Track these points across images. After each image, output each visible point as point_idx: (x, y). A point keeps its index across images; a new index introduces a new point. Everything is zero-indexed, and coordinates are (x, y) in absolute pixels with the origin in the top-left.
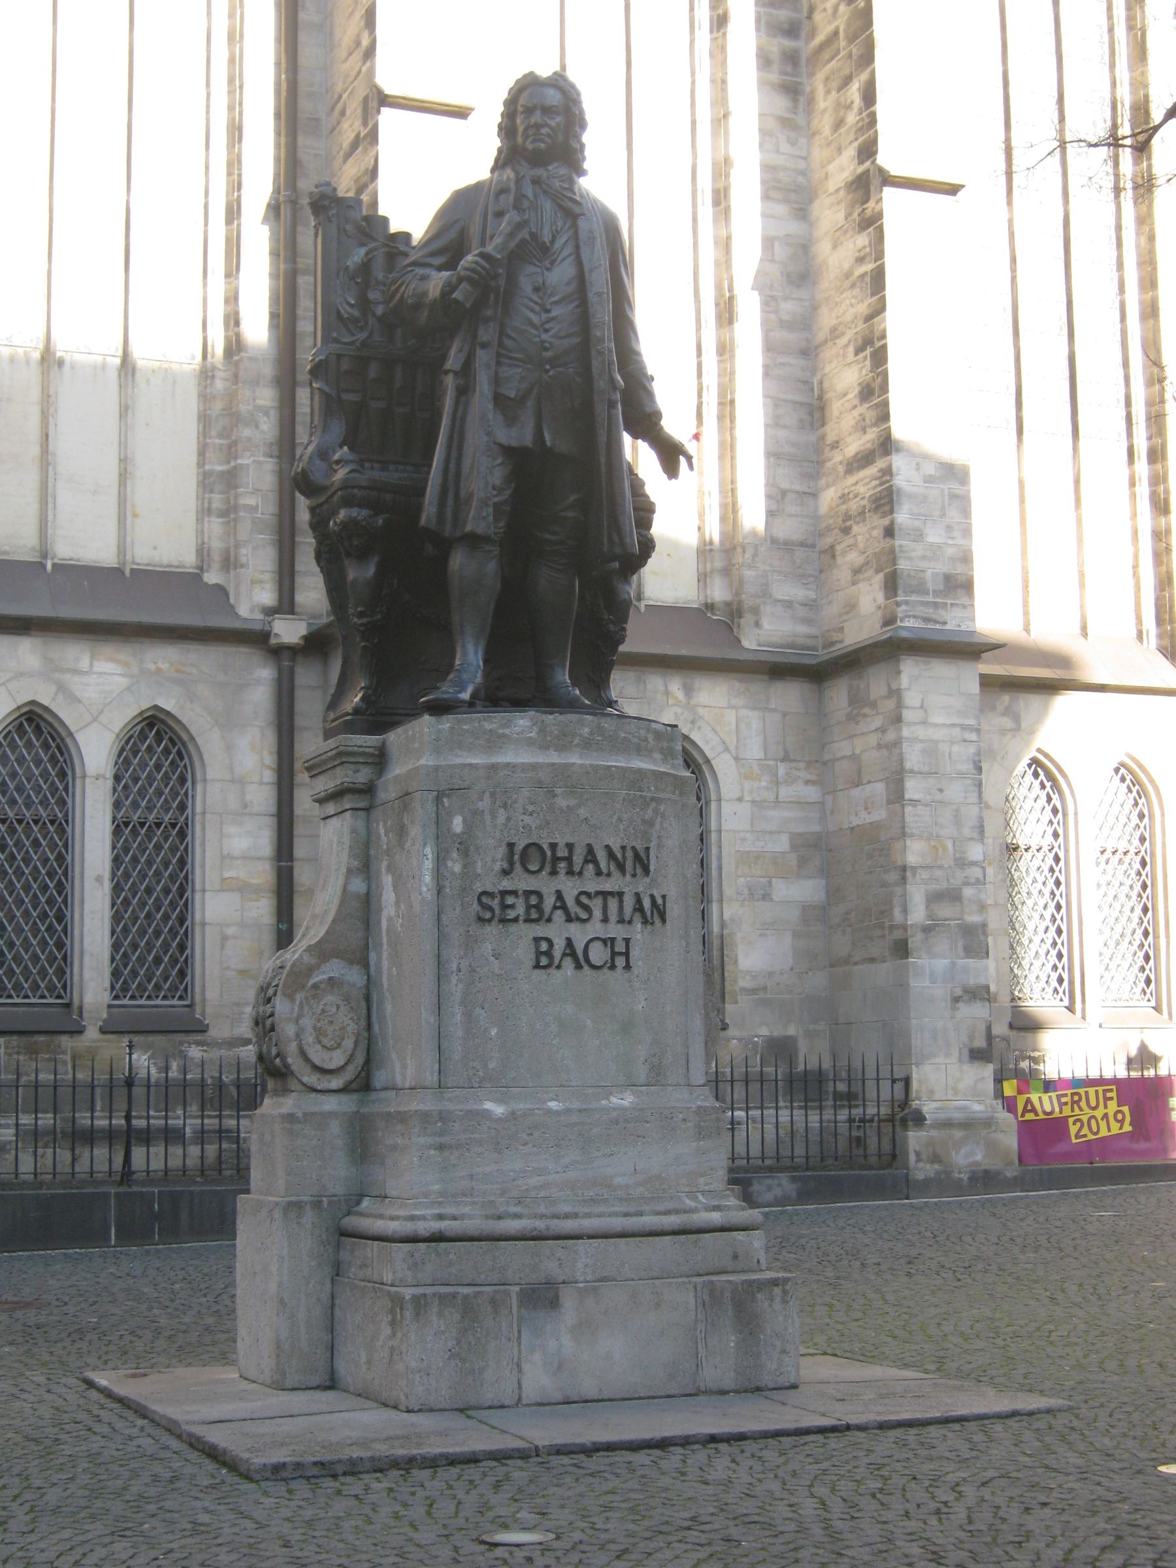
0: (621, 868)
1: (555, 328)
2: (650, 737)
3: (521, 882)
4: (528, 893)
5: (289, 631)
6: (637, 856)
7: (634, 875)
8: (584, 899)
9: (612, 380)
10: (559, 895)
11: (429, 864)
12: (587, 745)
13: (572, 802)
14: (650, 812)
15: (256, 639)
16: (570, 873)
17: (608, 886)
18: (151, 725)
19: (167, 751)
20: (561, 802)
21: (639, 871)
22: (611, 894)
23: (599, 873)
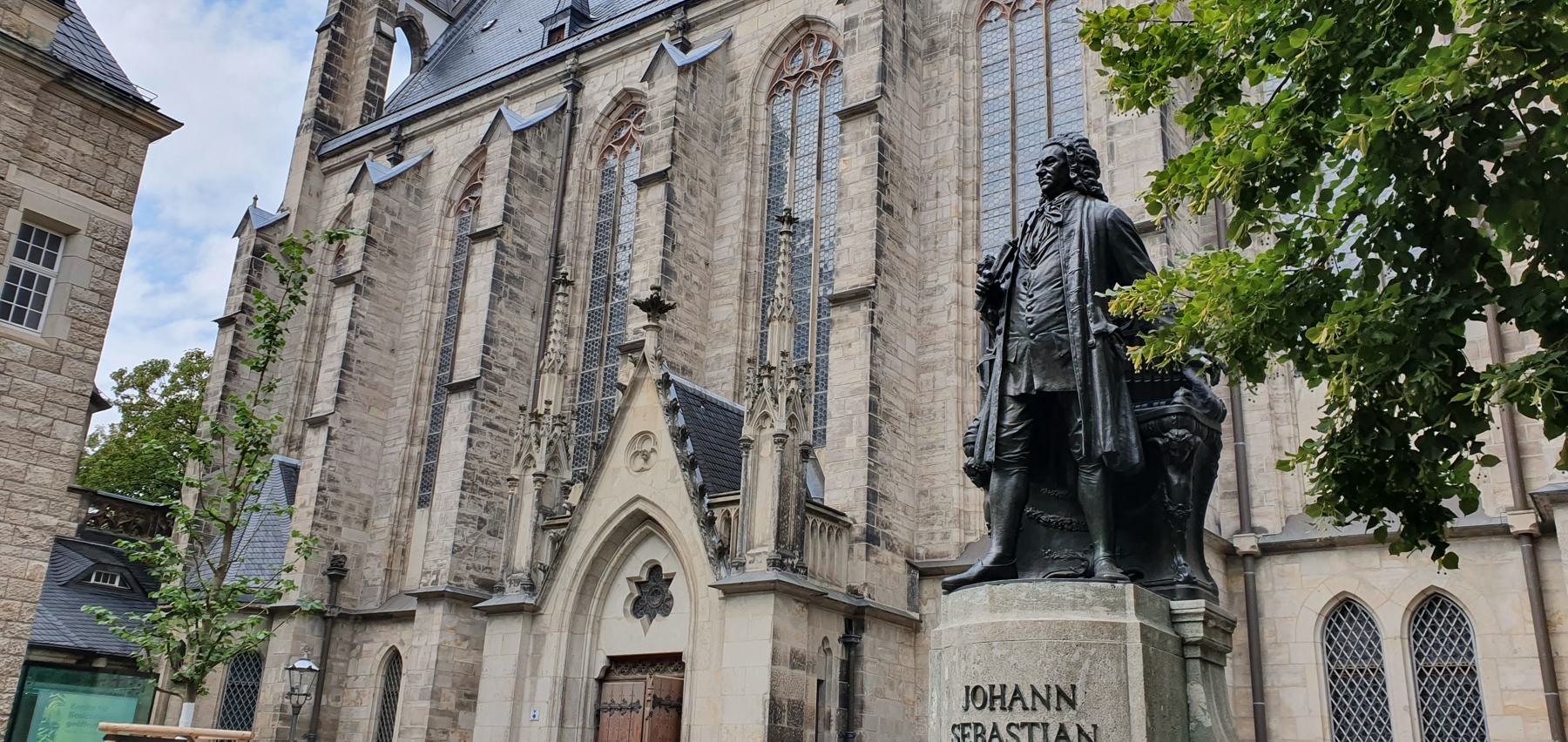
0: (1047, 704)
1: (1036, 306)
2: (1089, 594)
3: (974, 716)
4: (977, 725)
5: (1524, 522)
6: (1060, 693)
7: (1058, 709)
8: (1013, 730)
9: (1085, 331)
10: (995, 728)
11: (935, 704)
12: (1023, 606)
13: (1005, 652)
14: (1076, 656)
15: (1503, 531)
16: (1003, 708)
17: (1032, 718)
18: (1437, 600)
19: (1451, 618)
20: (997, 652)
21: (1064, 705)
22: (1033, 724)
23: (1025, 708)
